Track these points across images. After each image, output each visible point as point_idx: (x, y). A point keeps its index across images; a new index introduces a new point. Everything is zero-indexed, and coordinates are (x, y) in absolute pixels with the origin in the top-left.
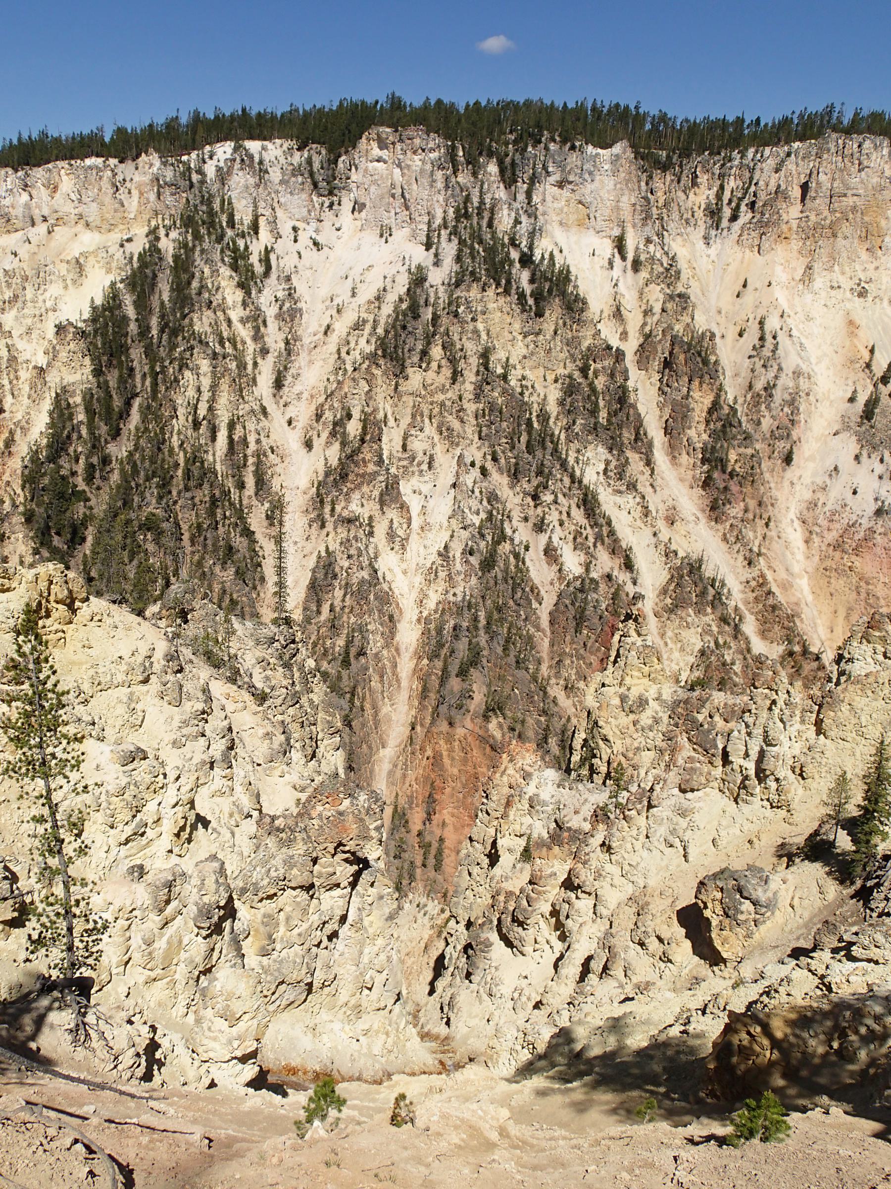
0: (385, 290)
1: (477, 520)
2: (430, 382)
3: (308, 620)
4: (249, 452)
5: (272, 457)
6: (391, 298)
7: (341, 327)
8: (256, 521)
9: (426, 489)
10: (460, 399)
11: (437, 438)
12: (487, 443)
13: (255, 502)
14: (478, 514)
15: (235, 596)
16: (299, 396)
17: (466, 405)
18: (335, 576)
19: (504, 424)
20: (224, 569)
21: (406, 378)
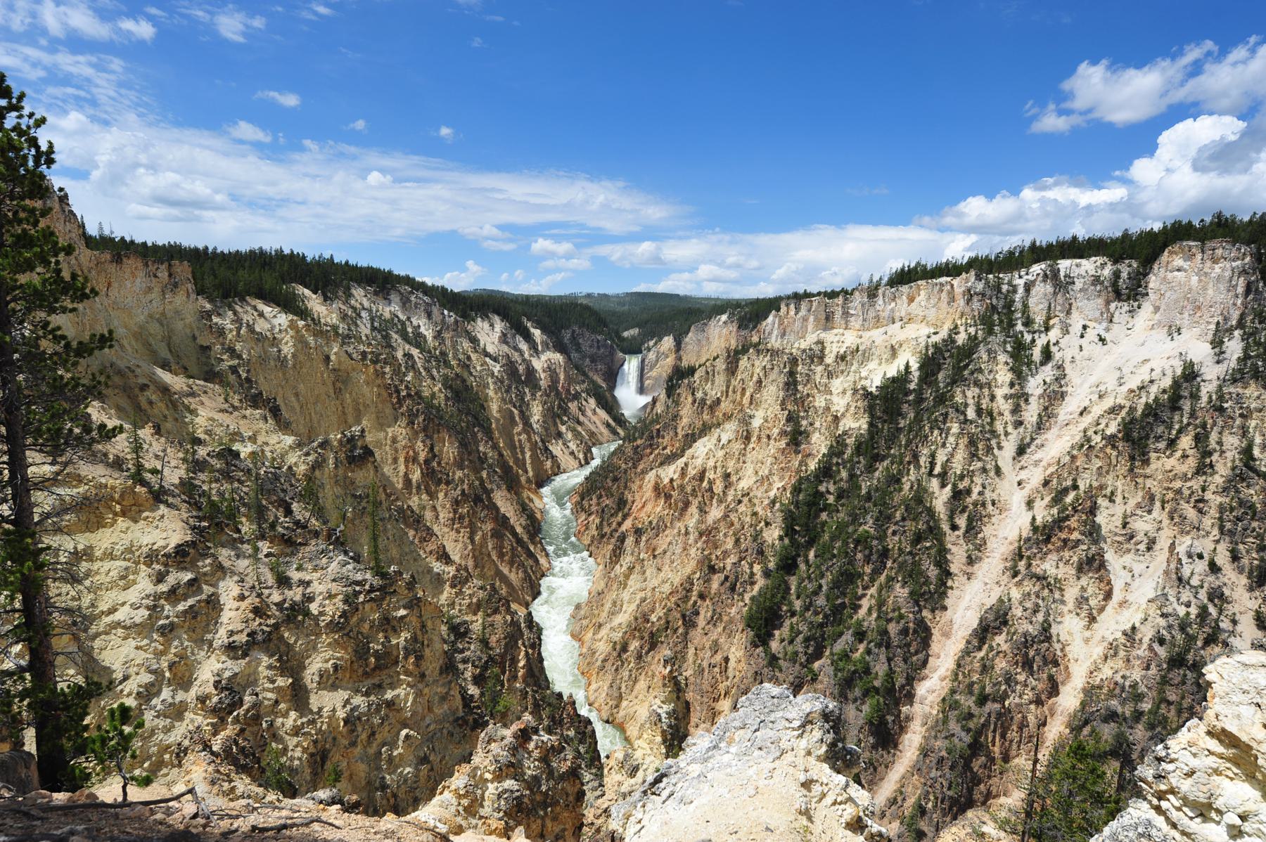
0: (1152, 382)
1: (1182, 611)
2: (1169, 468)
3: (967, 652)
4: (969, 500)
5: (990, 507)
6: (1154, 390)
7: (1097, 410)
8: (957, 560)
9: (1138, 568)
10: (1204, 490)
11: (1166, 522)
12: (1227, 539)
13: (962, 541)
14: (1188, 605)
15: (903, 611)
16: (1037, 463)
17: (1208, 495)
18: (1005, 623)
19: (1255, 524)
20: (903, 587)
21: (1146, 462)
